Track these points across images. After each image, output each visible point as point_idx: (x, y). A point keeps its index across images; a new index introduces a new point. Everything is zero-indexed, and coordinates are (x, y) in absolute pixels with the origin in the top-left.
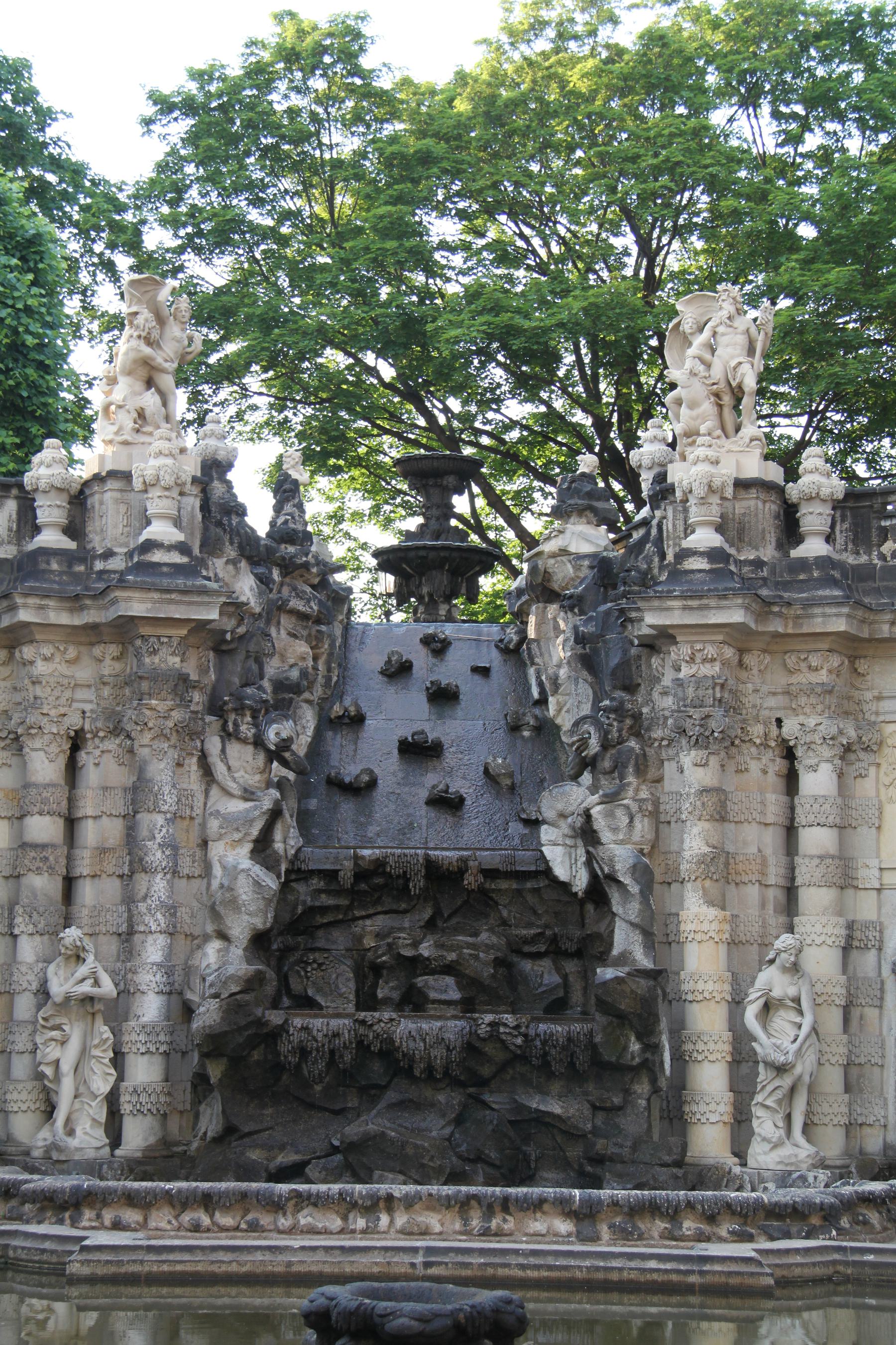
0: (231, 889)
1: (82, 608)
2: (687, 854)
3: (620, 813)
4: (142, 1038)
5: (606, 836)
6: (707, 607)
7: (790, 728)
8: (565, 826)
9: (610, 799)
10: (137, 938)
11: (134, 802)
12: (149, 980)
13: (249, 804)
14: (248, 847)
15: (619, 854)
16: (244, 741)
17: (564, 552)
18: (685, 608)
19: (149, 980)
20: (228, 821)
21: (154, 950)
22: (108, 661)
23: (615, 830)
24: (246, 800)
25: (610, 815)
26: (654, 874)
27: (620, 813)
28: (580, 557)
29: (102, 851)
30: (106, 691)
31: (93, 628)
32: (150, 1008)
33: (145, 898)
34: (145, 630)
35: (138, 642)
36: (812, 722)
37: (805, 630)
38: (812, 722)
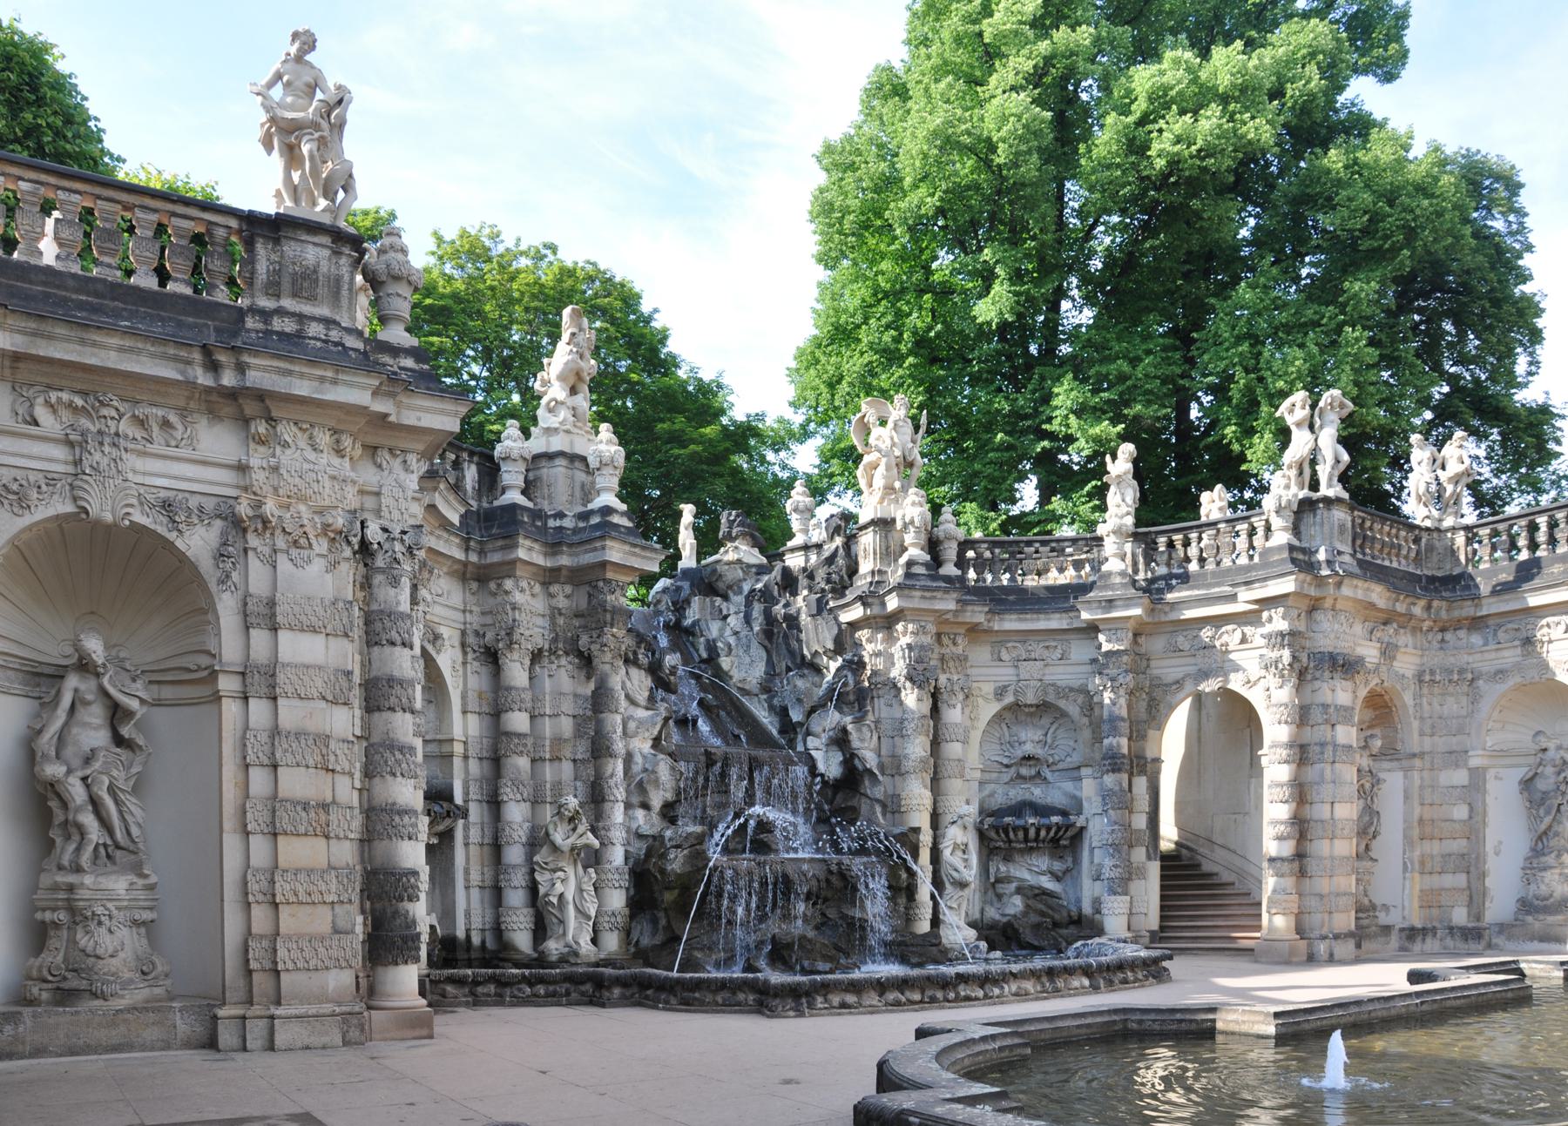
0: (654, 772)
1: (554, 554)
2: (913, 757)
3: (865, 729)
4: (617, 876)
5: (855, 743)
6: (934, 598)
7: (943, 679)
8: (824, 738)
9: (858, 721)
10: (607, 806)
11: (594, 705)
12: (618, 835)
13: (650, 713)
14: (650, 743)
15: (869, 757)
16: (639, 667)
17: (739, 561)
18: (923, 597)
19: (618, 835)
20: (641, 723)
21: (617, 814)
22: (561, 598)
23: (862, 740)
24: (647, 709)
25: (859, 730)
26: (895, 767)
27: (865, 729)
28: (749, 566)
29: (558, 741)
30: (561, 621)
31: (558, 569)
32: (617, 856)
33: (612, 776)
34: (610, 575)
35: (601, 584)
36: (956, 678)
37: (960, 619)
38: (956, 678)
